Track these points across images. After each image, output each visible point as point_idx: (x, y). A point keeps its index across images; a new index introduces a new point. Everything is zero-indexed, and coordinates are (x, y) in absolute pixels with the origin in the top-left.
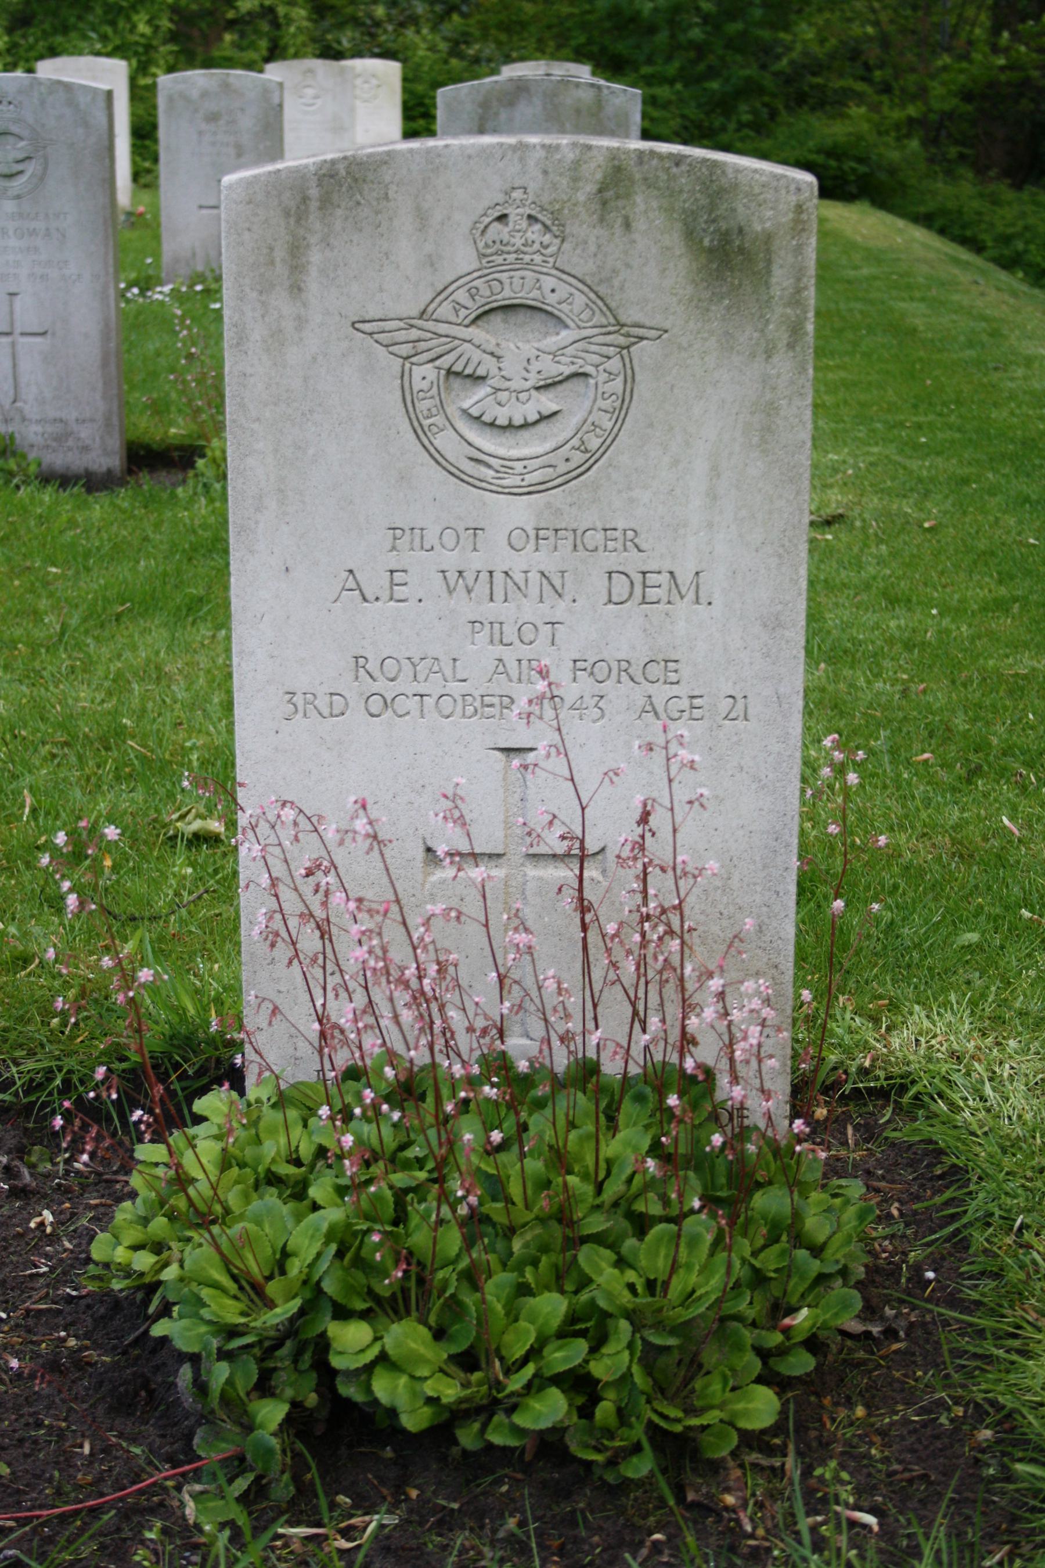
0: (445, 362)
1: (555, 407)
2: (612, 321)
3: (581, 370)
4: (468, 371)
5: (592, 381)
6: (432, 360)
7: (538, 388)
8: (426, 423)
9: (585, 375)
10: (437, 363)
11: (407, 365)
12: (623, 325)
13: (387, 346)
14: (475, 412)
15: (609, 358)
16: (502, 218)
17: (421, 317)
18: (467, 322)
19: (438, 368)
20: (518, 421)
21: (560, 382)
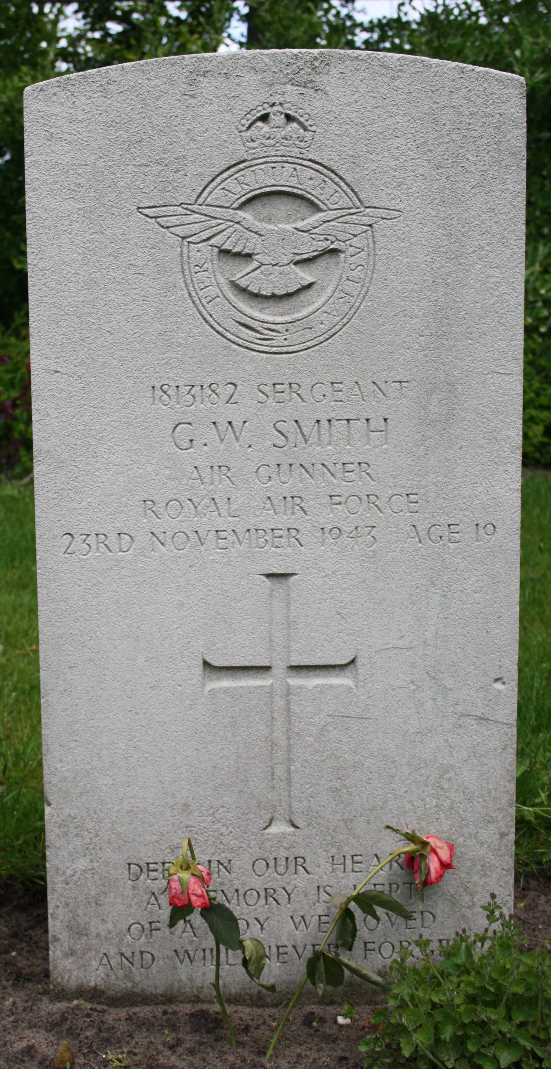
1: (310, 279)
2: (358, 203)
4: (236, 250)
5: (342, 255)
7: (296, 263)
10: (212, 242)
12: (367, 207)
13: (168, 227)
14: (243, 283)
15: (355, 236)
16: (264, 118)
19: (212, 246)
21: (315, 258)
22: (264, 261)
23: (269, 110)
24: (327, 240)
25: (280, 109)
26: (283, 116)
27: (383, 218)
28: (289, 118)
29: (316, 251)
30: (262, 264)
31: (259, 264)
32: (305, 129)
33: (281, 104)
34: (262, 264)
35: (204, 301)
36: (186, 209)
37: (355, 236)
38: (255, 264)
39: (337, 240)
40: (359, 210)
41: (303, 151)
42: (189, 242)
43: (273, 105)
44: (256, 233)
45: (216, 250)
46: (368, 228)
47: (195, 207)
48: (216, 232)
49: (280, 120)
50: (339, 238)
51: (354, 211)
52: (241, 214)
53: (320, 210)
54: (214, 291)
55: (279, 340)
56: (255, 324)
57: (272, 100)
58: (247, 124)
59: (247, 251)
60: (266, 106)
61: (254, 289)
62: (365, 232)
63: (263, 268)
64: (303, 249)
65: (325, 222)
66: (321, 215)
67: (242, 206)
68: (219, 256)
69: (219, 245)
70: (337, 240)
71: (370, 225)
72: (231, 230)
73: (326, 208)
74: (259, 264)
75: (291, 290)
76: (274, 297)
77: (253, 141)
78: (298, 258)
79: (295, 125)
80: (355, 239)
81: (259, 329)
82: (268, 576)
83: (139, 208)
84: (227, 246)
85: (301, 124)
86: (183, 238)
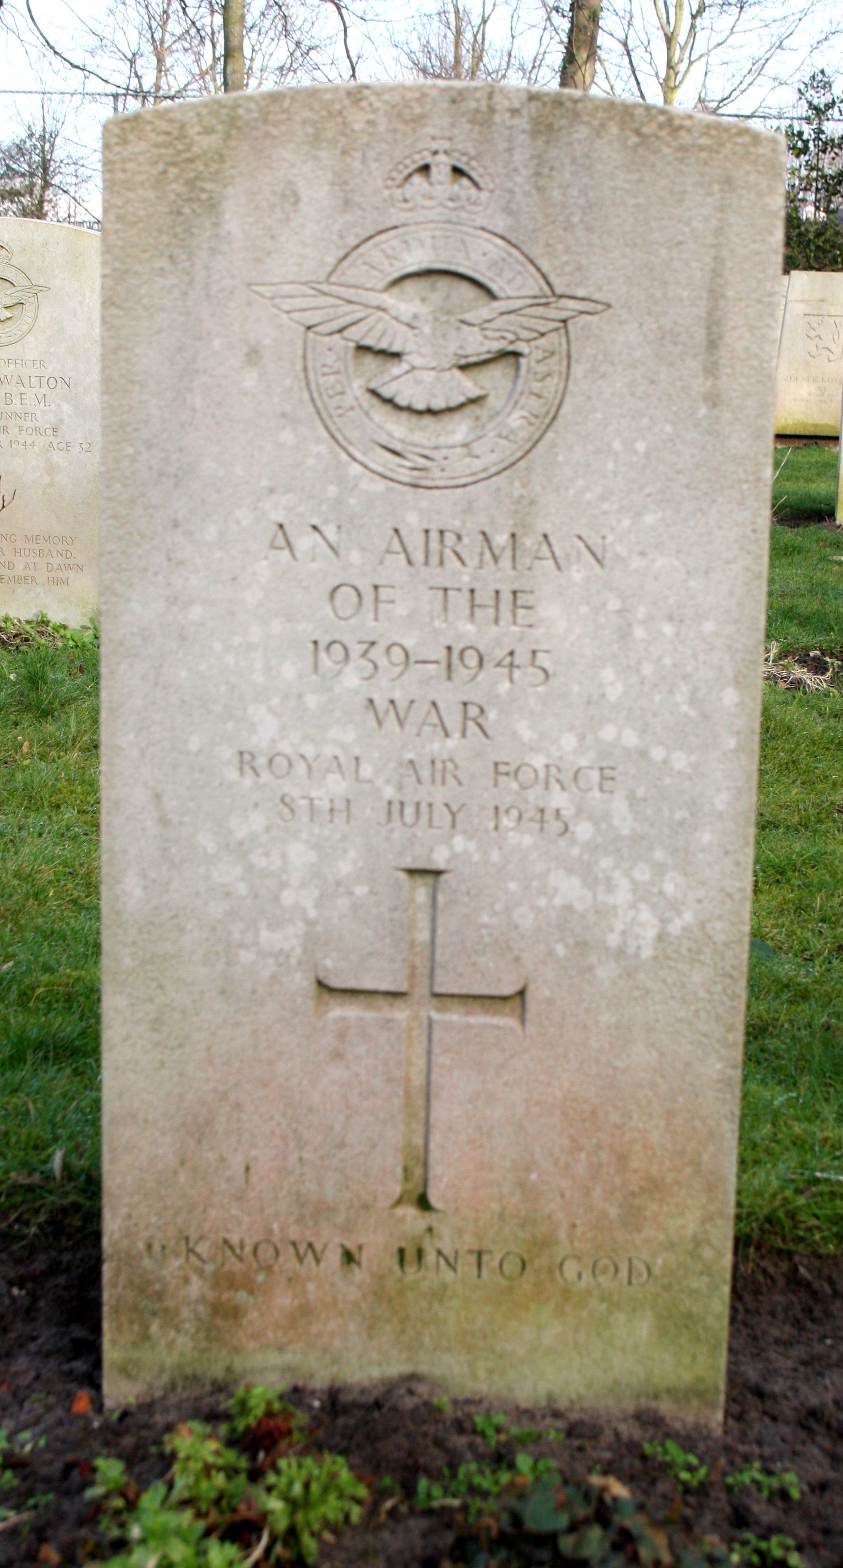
0: (355, 333)
2: (549, 293)
3: (511, 348)
6: (341, 331)
8: (333, 403)
9: (516, 355)
10: (346, 333)
12: (561, 296)
14: (386, 392)
15: (543, 335)
16: (425, 169)
17: (327, 281)
20: (438, 404)
23: (429, 160)
24: (504, 338)
26: (448, 169)
29: (489, 352)
30: (413, 368)
34: (413, 368)
36: (313, 289)
37: (543, 335)
38: (405, 366)
39: (518, 339)
41: (473, 217)
42: (317, 333)
43: (435, 153)
45: (352, 345)
46: (561, 325)
47: (325, 288)
51: (543, 301)
52: (388, 299)
57: (435, 146)
58: (400, 177)
60: (426, 153)
61: (402, 401)
62: (557, 329)
63: (416, 372)
64: (469, 350)
65: (502, 314)
66: (495, 304)
68: (356, 357)
69: (357, 338)
70: (518, 339)
72: (371, 321)
75: (453, 404)
76: (430, 412)
77: (406, 200)
78: (463, 362)
79: (465, 182)
83: (249, 285)
84: (368, 342)
85: (470, 178)
86: (309, 328)
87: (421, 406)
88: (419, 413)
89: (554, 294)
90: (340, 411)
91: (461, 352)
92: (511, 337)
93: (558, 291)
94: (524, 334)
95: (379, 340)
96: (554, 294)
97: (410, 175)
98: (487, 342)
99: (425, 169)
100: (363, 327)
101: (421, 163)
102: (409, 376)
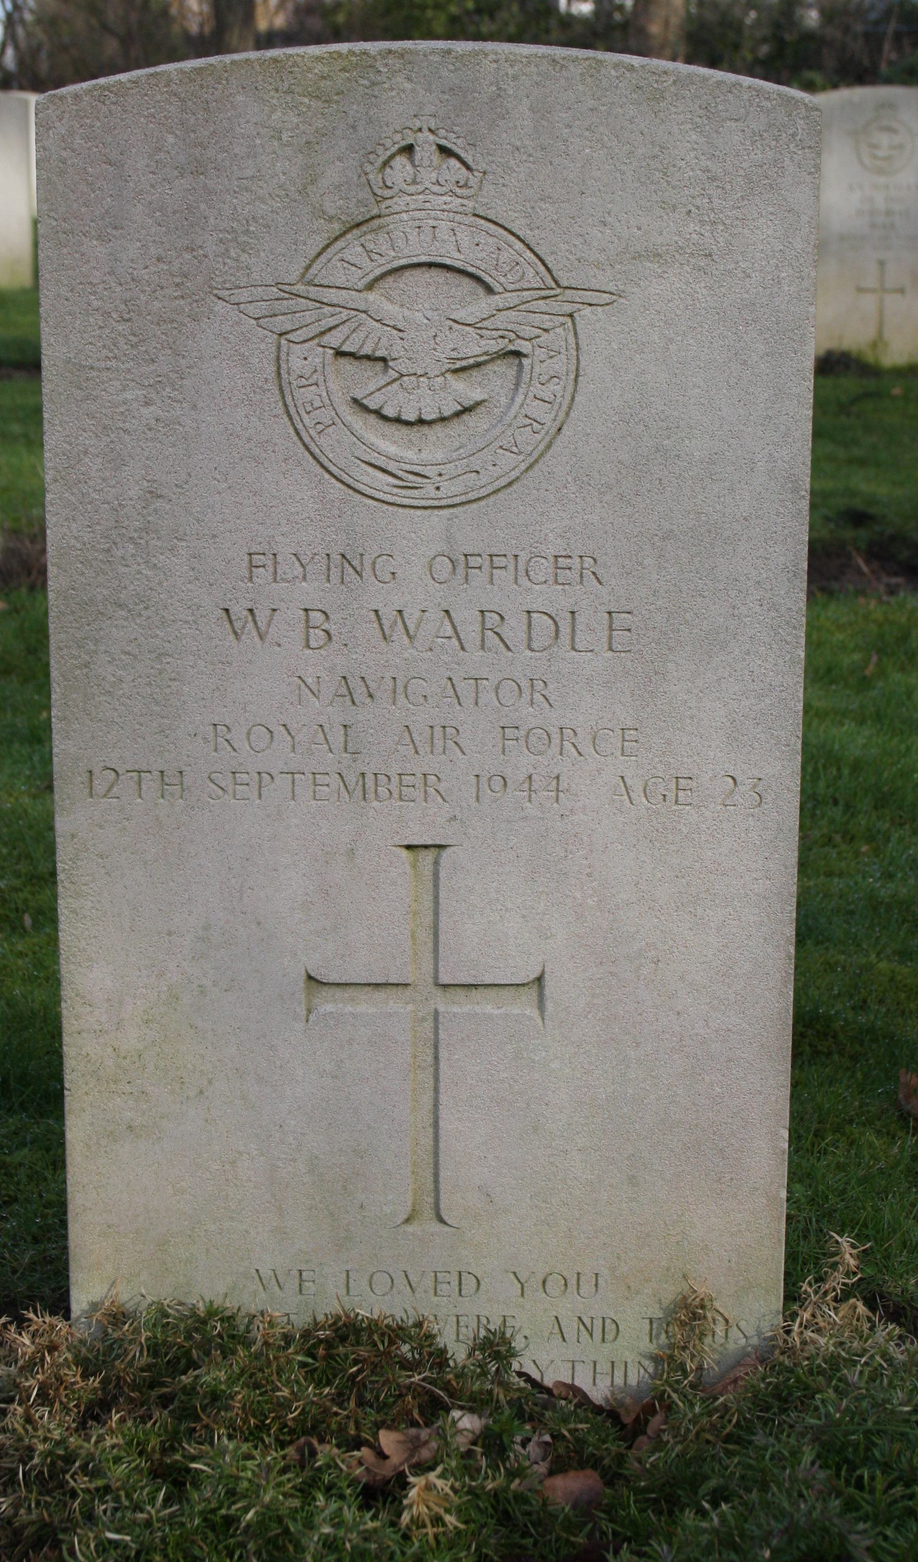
0: (334, 339)
4: (363, 352)
5: (526, 362)
7: (456, 371)
9: (517, 354)
10: (326, 339)
11: (283, 342)
14: (372, 404)
15: (545, 330)
18: (361, 285)
22: (404, 371)
23: (410, 141)
24: (502, 337)
25: (431, 137)
26: (434, 147)
27: (590, 305)
28: (444, 151)
29: (486, 353)
30: (402, 376)
31: (397, 375)
32: (468, 168)
33: (430, 130)
34: (402, 376)
35: (312, 432)
36: (285, 292)
37: (545, 330)
38: (393, 374)
39: (518, 337)
40: (552, 293)
41: (465, 202)
44: (394, 327)
46: (569, 320)
47: (300, 288)
48: (331, 325)
49: (426, 152)
50: (521, 334)
53: (489, 290)
54: (326, 415)
55: (430, 491)
56: (392, 466)
59: (379, 354)
61: (390, 412)
67: (370, 287)
69: (335, 344)
71: (571, 316)
73: (501, 290)
74: (397, 375)
78: (459, 364)
79: (453, 162)
80: (545, 335)
81: (400, 473)
82: (409, 847)
86: (281, 335)
87: (412, 417)
88: (407, 423)
89: (559, 286)
90: (320, 427)
91: (454, 354)
92: (513, 336)
93: (565, 283)
94: (528, 331)
95: (362, 346)
96: (559, 286)
97: (392, 157)
98: (483, 343)
99: (409, 150)
100: (345, 330)
101: (403, 143)
102: (398, 383)
